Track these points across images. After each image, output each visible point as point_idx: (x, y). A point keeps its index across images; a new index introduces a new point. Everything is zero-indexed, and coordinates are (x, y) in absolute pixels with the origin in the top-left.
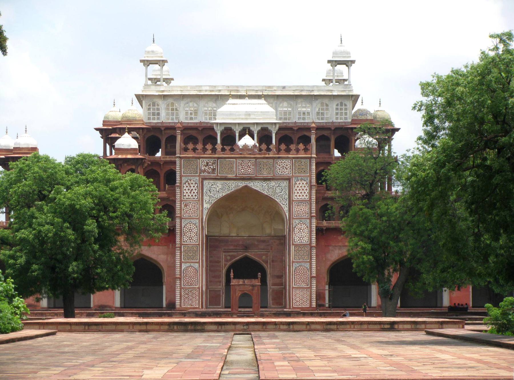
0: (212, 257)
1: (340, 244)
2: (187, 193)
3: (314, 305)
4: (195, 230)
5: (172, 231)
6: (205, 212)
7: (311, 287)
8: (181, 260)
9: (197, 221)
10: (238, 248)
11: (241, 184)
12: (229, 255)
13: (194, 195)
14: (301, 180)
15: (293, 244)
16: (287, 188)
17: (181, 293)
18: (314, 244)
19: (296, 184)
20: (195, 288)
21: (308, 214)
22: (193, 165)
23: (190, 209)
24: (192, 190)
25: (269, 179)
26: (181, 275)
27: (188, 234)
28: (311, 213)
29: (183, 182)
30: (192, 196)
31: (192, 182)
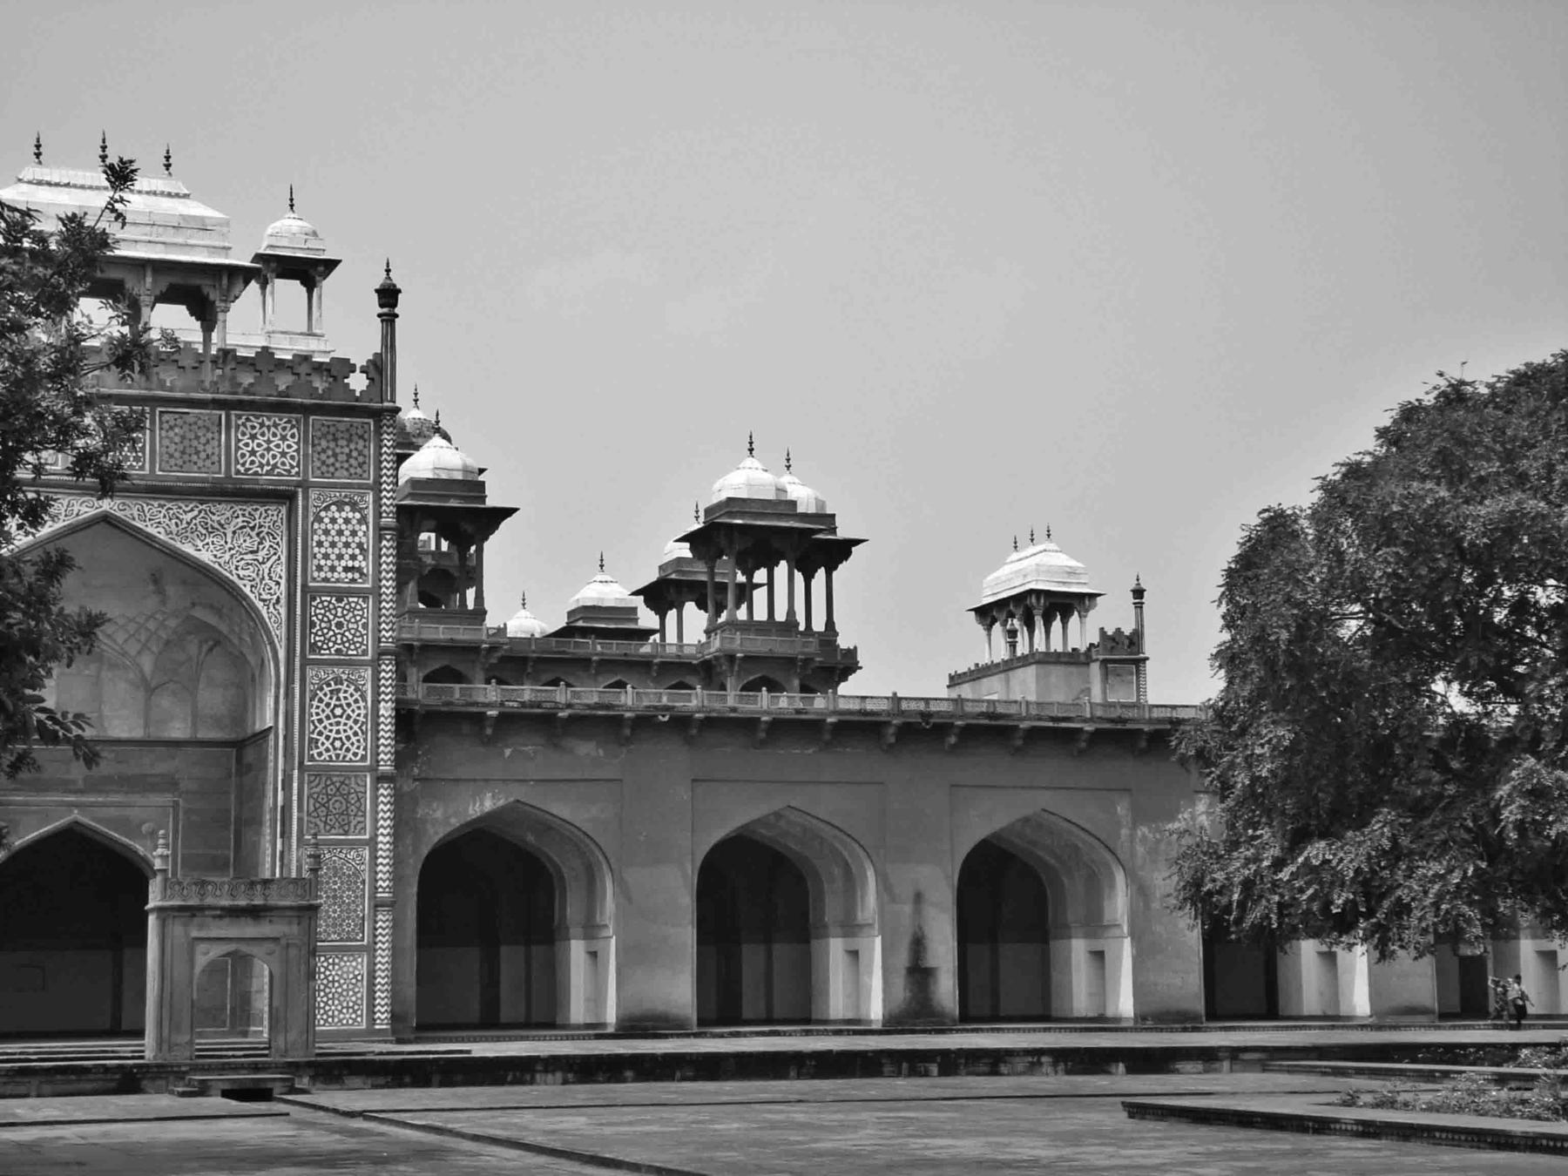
18: (386, 767)
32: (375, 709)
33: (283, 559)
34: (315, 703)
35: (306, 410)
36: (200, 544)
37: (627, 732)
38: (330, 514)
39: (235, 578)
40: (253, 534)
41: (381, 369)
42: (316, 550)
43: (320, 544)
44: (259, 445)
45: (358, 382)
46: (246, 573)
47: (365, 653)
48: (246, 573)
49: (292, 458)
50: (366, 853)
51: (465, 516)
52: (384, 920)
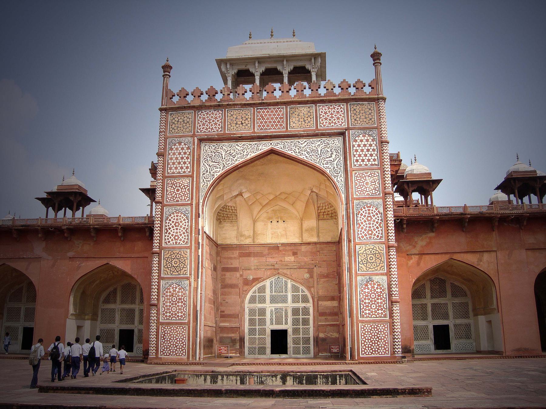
6: (202, 194)
11: (264, 147)
18: (393, 242)
26: (158, 300)
27: (173, 231)
32: (386, 216)
34: (359, 216)
35: (346, 101)
36: (308, 156)
37: (497, 224)
38: (360, 138)
41: (375, 85)
43: (356, 151)
44: (328, 116)
45: (367, 90)
46: (327, 166)
47: (379, 194)
48: (327, 166)
49: (342, 119)
50: (385, 278)
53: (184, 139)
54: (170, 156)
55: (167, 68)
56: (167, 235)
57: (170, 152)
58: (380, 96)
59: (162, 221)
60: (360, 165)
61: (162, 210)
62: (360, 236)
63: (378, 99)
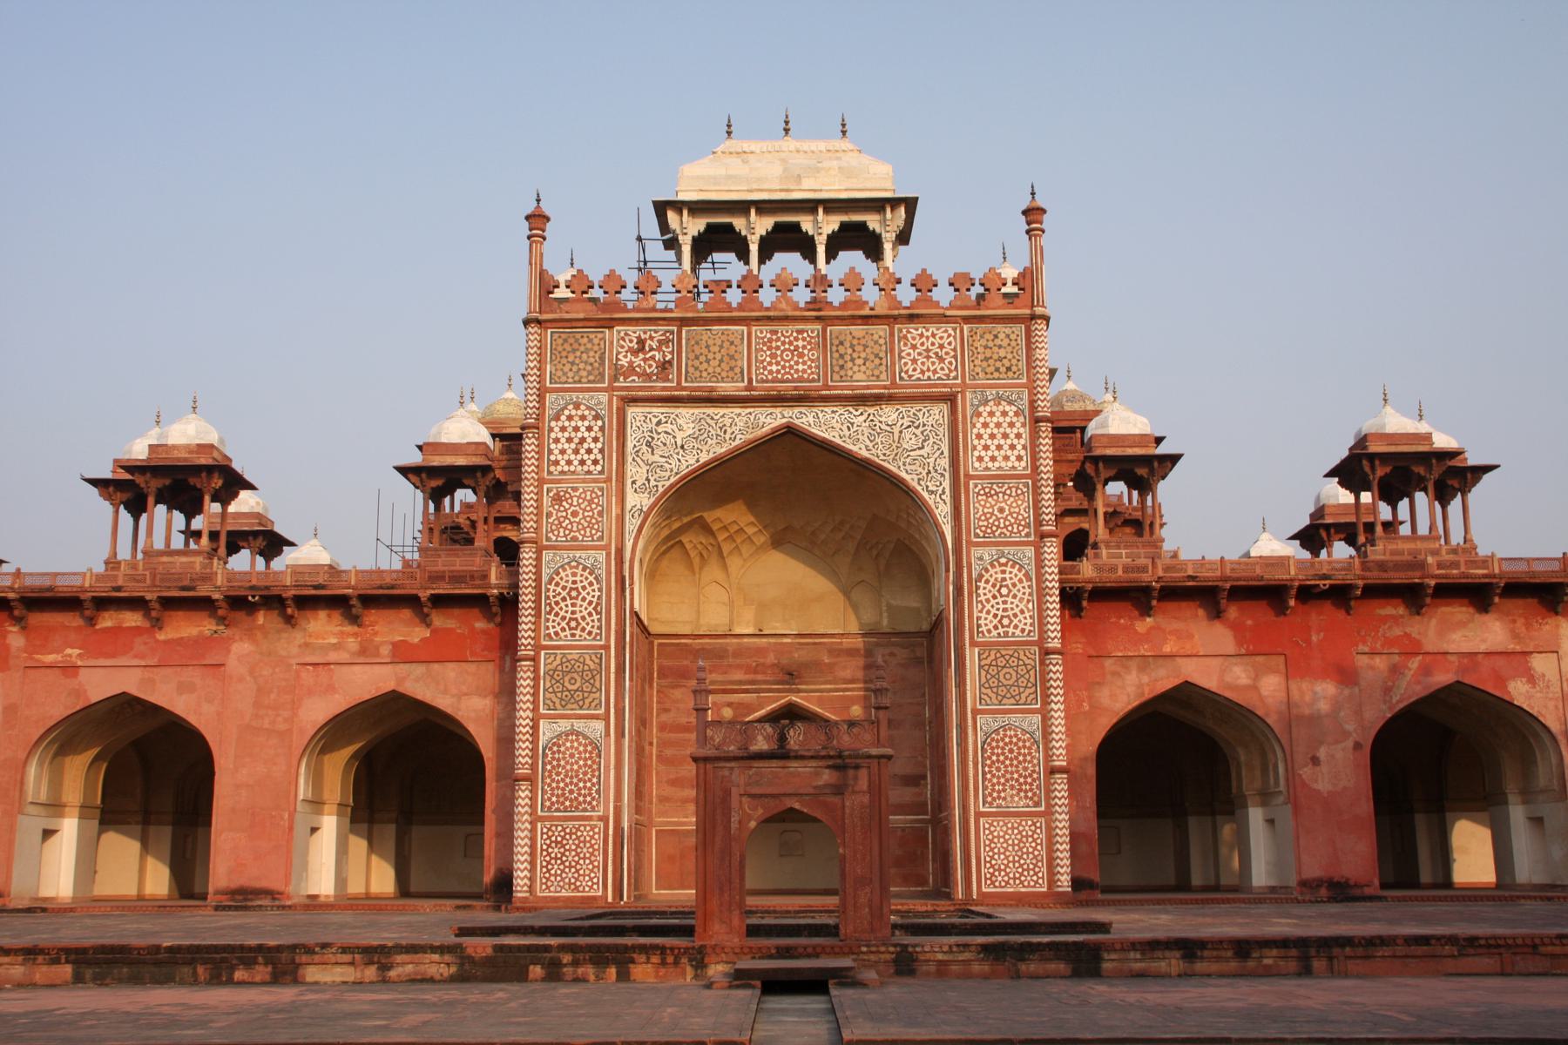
0: (666, 710)
1: (1144, 650)
2: (563, 452)
3: (1064, 882)
4: (592, 594)
5: (509, 604)
6: (632, 525)
7: (1049, 813)
8: (535, 709)
9: (601, 556)
10: (760, 677)
11: (770, 419)
12: (730, 705)
13: (589, 459)
14: (998, 400)
15: (973, 644)
16: (944, 431)
17: (533, 839)
19: (979, 415)
20: (589, 818)
21: (1028, 525)
22: (587, 351)
23: (575, 514)
24: (583, 440)
25: (877, 400)
26: (534, 766)
27: (565, 609)
28: (1039, 523)
29: (549, 413)
30: (582, 462)
31: (583, 410)
33: (946, 453)
34: (982, 584)
39: (903, 475)
40: (918, 432)
41: (1028, 280)
42: (976, 442)
47: (1028, 535)
51: (1145, 467)
52: (1061, 785)
53: (587, 395)
54: (553, 435)
55: (537, 220)
56: (552, 617)
57: (553, 424)
58: (1039, 310)
59: (538, 587)
60: (987, 469)
61: (539, 559)
62: (984, 629)
63: (1033, 317)
